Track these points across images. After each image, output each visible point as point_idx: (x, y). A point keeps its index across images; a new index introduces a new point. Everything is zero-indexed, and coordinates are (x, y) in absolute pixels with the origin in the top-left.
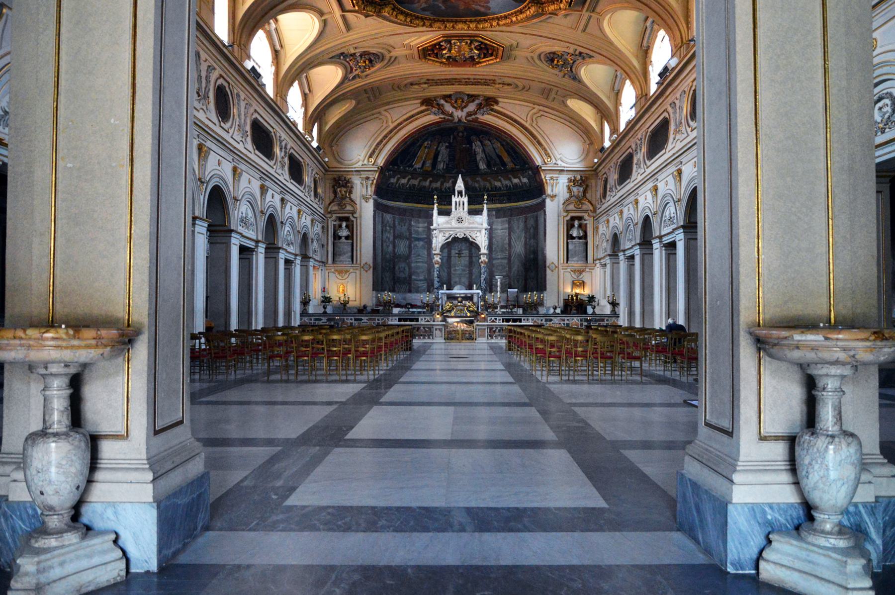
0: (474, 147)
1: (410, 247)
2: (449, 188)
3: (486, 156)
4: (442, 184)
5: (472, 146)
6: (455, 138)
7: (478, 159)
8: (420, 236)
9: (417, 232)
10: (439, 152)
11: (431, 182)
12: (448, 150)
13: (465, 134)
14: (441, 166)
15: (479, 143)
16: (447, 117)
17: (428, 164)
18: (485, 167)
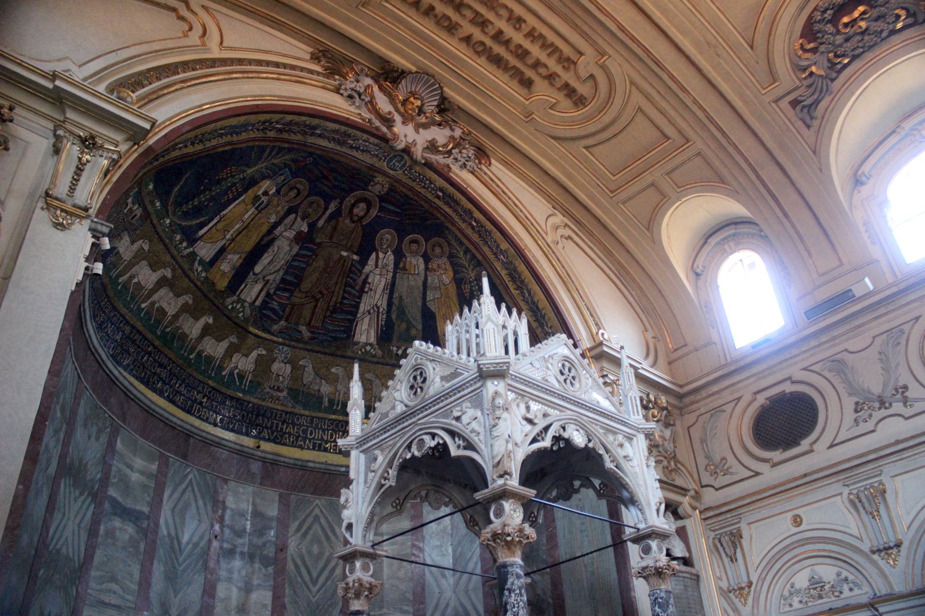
0: (367, 269)
1: (93, 532)
2: (241, 376)
3: (390, 304)
4: (229, 353)
5: (363, 262)
6: (337, 214)
7: (362, 308)
8: (129, 504)
9: (126, 486)
10: (273, 241)
11: (206, 331)
12: (296, 249)
13: (374, 212)
14: (252, 292)
15: (391, 257)
16: (377, 123)
17: (227, 266)
18: (372, 340)
